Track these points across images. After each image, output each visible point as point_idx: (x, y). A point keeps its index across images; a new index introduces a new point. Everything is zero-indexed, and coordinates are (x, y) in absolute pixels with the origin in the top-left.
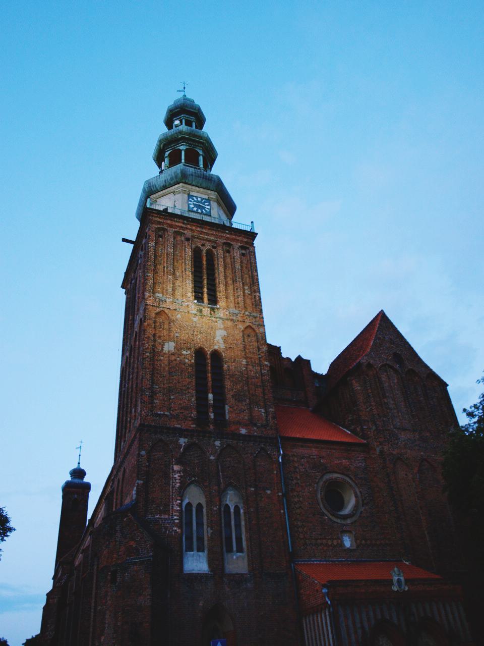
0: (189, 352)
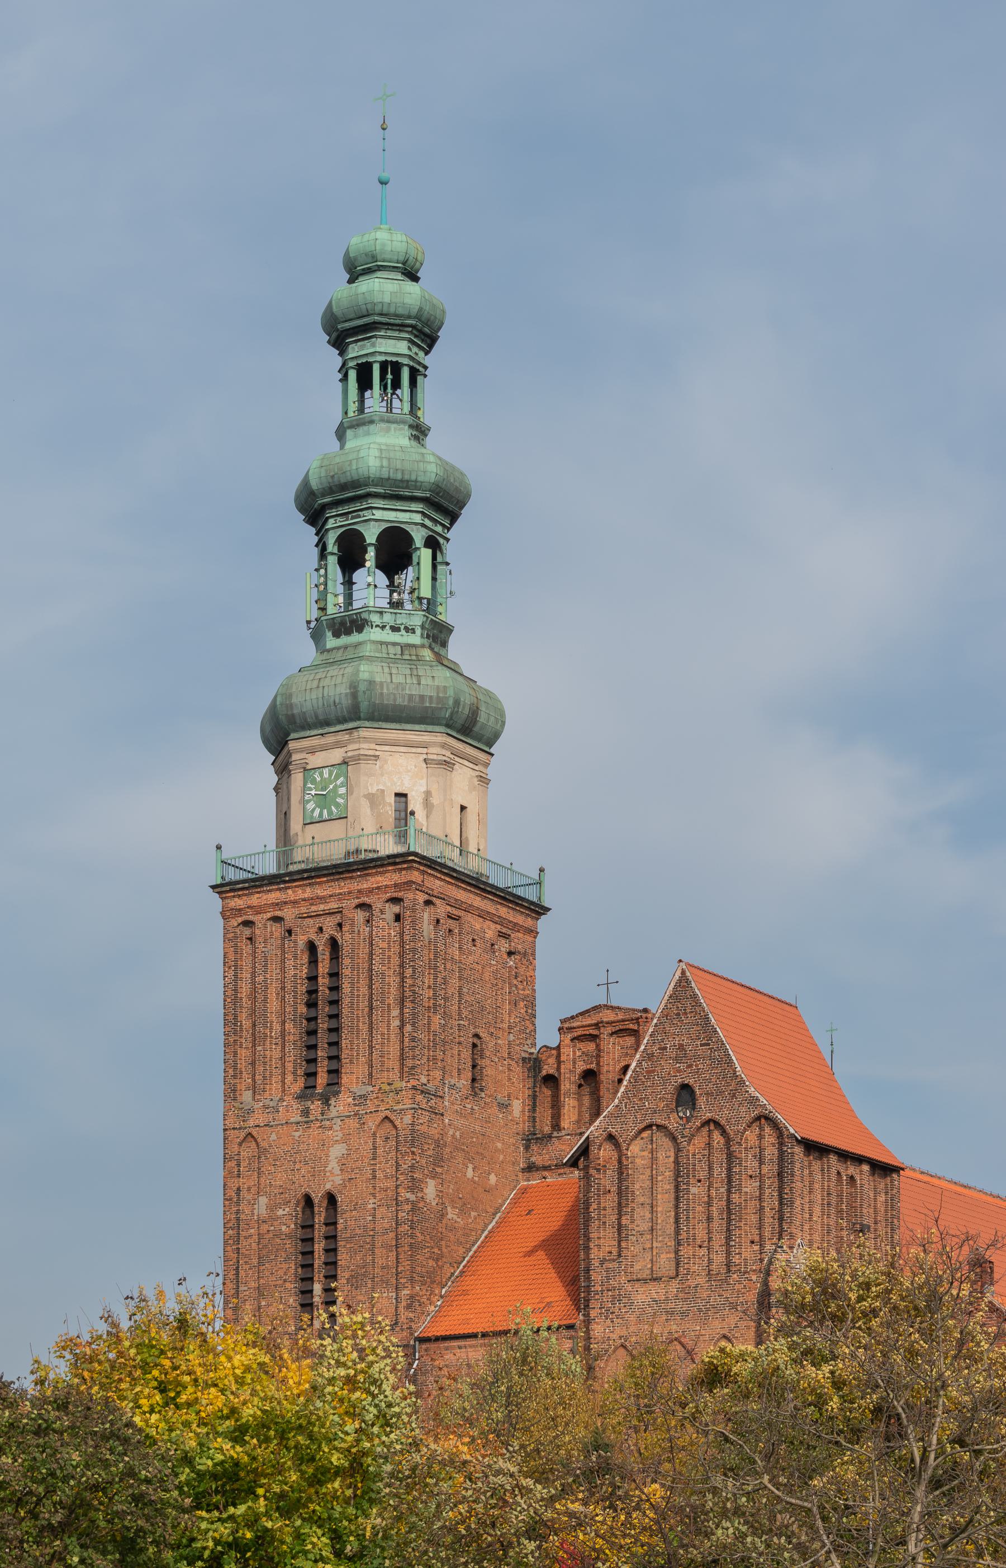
0: (287, 1209)
